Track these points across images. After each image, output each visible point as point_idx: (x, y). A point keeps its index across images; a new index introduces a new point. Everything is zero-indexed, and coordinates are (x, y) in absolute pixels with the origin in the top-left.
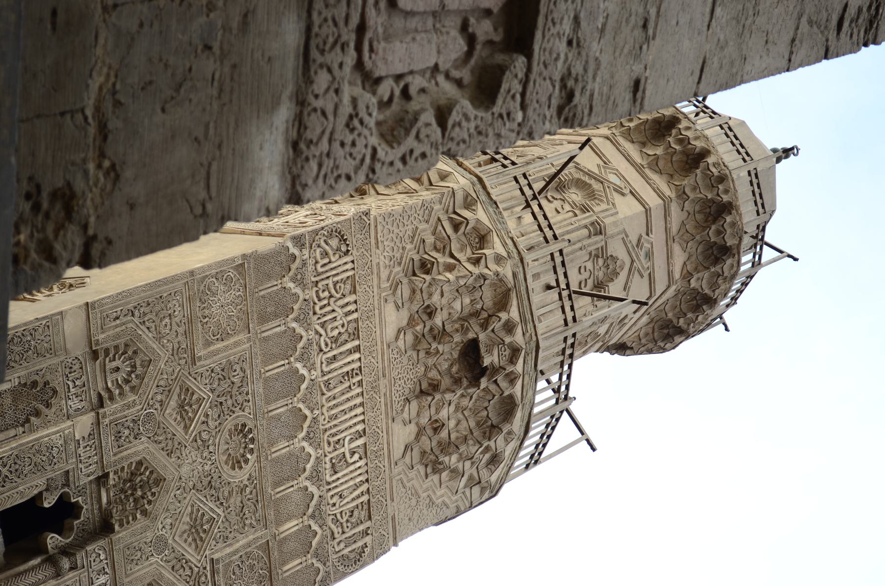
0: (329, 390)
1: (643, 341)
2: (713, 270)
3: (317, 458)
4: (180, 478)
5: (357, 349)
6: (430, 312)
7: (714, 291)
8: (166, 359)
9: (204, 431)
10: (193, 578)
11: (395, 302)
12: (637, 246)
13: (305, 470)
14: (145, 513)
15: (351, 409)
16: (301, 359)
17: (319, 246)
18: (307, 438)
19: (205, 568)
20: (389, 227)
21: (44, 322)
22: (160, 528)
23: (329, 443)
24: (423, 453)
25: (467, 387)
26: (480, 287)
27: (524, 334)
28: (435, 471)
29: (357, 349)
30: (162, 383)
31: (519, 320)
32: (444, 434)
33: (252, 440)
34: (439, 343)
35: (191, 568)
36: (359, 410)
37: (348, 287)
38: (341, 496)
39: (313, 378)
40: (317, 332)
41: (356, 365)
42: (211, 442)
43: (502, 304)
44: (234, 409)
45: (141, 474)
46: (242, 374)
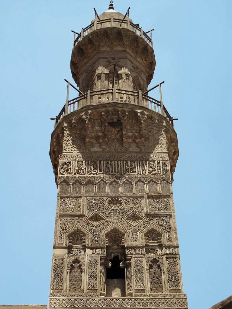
0: (109, 171)
4: (117, 223)
5: (100, 162)
9: (106, 214)
11: (91, 148)
12: (109, 62)
15: (118, 165)
20: (68, 148)
21: (54, 261)
22: (129, 230)
25: (123, 125)
27: (110, 107)
28: (148, 138)
29: (100, 162)
30: (86, 226)
31: (105, 109)
32: (137, 134)
35: (146, 222)
36: (119, 162)
37: (80, 163)
38: (144, 170)
40: (90, 175)
41: (105, 162)
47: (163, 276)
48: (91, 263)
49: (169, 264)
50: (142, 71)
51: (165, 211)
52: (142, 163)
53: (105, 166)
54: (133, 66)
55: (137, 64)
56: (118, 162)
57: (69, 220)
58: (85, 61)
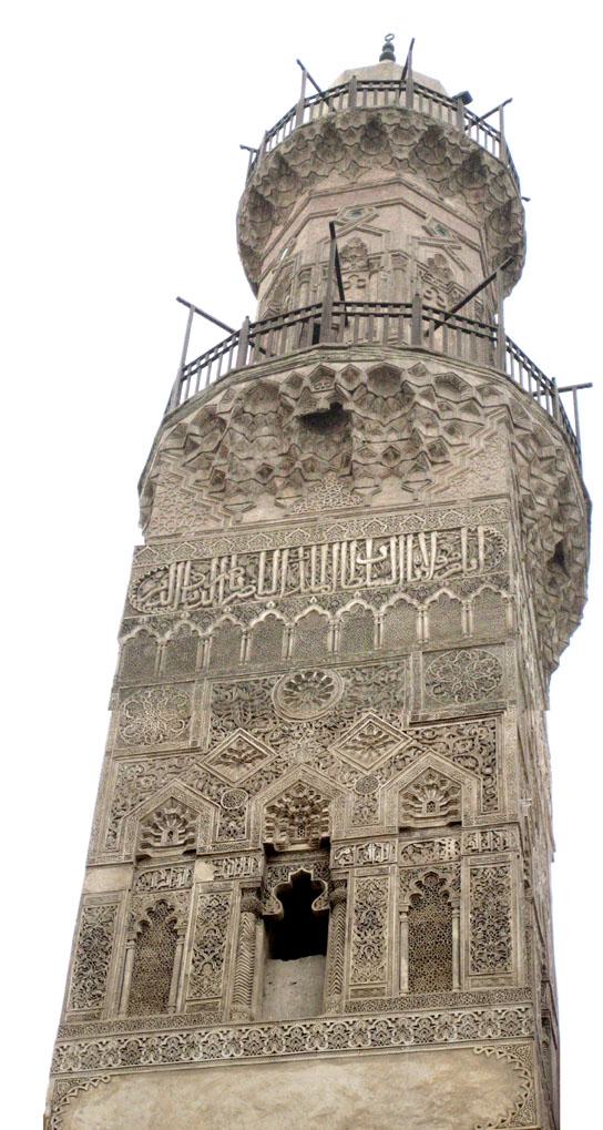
1: (483, 199)
2: (390, 136)
3: (363, 597)
4: (308, 763)
6: (266, 471)
7: (418, 131)
8: (179, 781)
10: (421, 746)
11: (243, 512)
13: (369, 611)
14: (326, 803)
16: (247, 619)
17: (144, 603)
18: (333, 609)
19: (417, 732)
21: (83, 913)
23: (355, 582)
24: (417, 468)
26: (254, 416)
28: (442, 453)
29: (270, 553)
30: (200, 785)
31: (290, 373)
32: (401, 446)
33: (309, 674)
34: (297, 459)
35: (410, 749)
36: (336, 547)
39: (274, 605)
42: (287, 729)
43: (273, 390)
44: (265, 698)
45: (287, 807)
46: (234, 689)
47: (455, 934)
48: (208, 909)
49: (478, 888)
50: (463, 240)
51: (484, 700)
52: (413, 542)
53: (284, 567)
54: (424, 227)
55: (444, 218)
56: (331, 545)
57: (145, 772)
58: (277, 231)
